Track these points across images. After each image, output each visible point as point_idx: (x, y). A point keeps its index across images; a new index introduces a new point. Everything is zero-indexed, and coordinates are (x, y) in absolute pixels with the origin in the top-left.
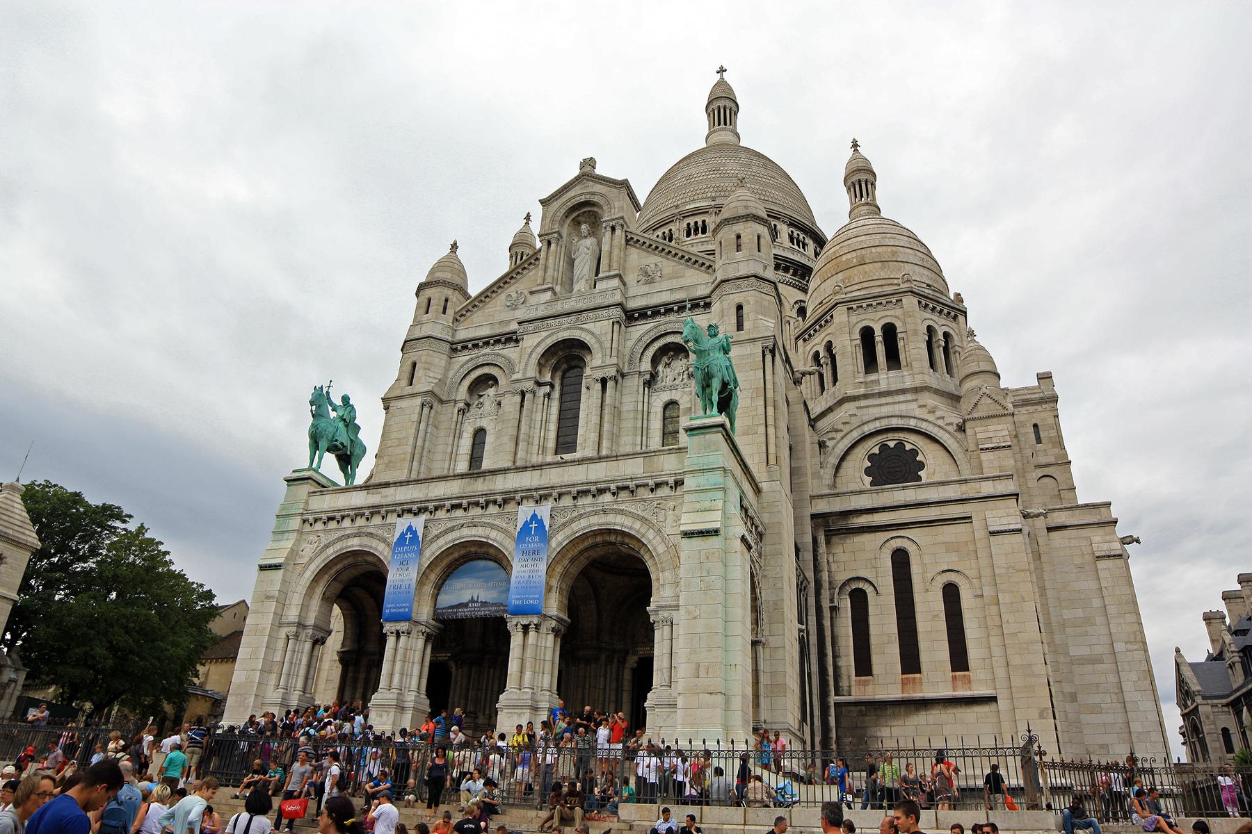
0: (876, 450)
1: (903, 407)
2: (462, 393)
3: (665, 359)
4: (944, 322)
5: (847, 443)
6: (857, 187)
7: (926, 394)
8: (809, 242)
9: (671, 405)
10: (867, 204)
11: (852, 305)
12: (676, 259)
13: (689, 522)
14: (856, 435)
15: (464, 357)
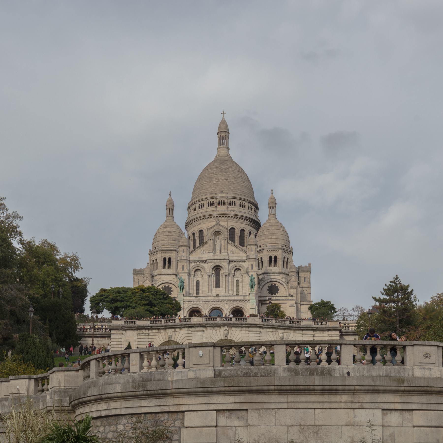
0: (270, 285)
1: (276, 276)
2: (193, 273)
3: (236, 271)
4: (288, 255)
5: (264, 283)
6: (271, 208)
7: (281, 274)
8: (253, 207)
9: (237, 280)
10: (273, 214)
11: (269, 249)
12: (239, 249)
13: (250, 306)
14: (266, 282)
15: (192, 264)
